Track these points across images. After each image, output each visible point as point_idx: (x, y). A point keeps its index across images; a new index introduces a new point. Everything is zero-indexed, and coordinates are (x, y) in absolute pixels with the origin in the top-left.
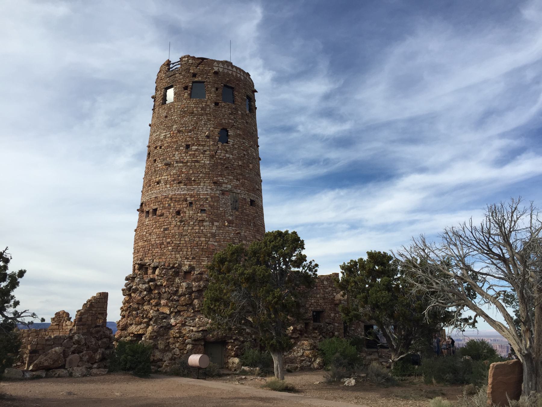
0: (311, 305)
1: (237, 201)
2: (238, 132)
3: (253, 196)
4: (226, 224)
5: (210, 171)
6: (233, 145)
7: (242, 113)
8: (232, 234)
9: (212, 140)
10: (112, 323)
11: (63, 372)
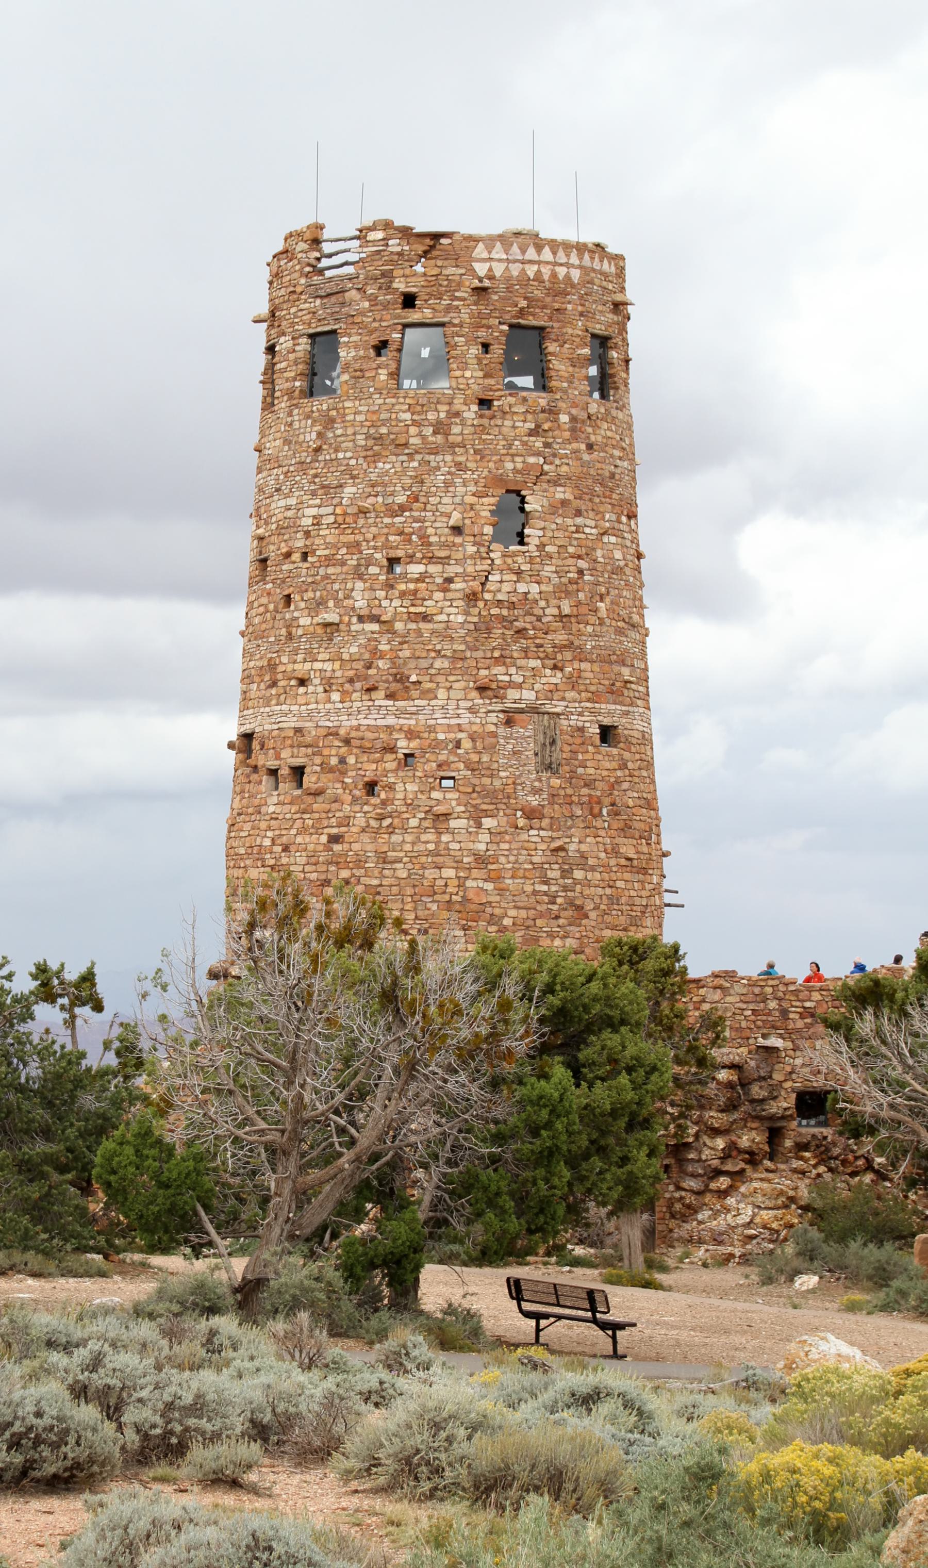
0: (790, 1073)
1: (553, 742)
2: (560, 493)
3: (610, 711)
4: (521, 822)
6: (541, 547)
7: (573, 419)
8: (540, 853)
9: (472, 539)
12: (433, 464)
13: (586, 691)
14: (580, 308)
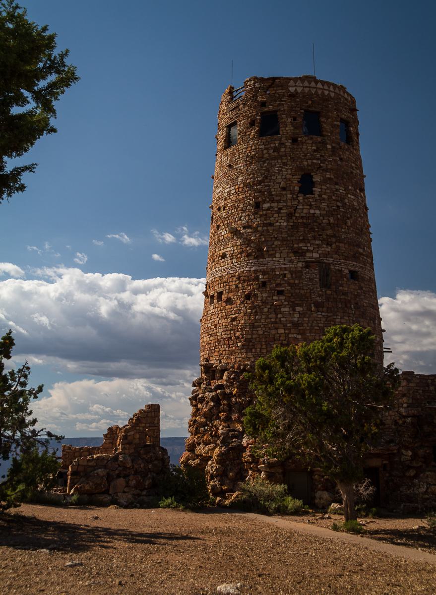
1: (327, 275)
3: (353, 265)
4: (313, 309)
5: (289, 236)
6: (320, 196)
7: (333, 147)
9: (290, 192)
10: (173, 440)
11: (107, 498)
12: (273, 164)
13: (343, 255)
14: (335, 107)
